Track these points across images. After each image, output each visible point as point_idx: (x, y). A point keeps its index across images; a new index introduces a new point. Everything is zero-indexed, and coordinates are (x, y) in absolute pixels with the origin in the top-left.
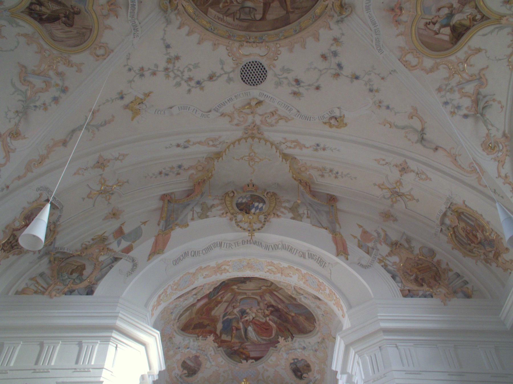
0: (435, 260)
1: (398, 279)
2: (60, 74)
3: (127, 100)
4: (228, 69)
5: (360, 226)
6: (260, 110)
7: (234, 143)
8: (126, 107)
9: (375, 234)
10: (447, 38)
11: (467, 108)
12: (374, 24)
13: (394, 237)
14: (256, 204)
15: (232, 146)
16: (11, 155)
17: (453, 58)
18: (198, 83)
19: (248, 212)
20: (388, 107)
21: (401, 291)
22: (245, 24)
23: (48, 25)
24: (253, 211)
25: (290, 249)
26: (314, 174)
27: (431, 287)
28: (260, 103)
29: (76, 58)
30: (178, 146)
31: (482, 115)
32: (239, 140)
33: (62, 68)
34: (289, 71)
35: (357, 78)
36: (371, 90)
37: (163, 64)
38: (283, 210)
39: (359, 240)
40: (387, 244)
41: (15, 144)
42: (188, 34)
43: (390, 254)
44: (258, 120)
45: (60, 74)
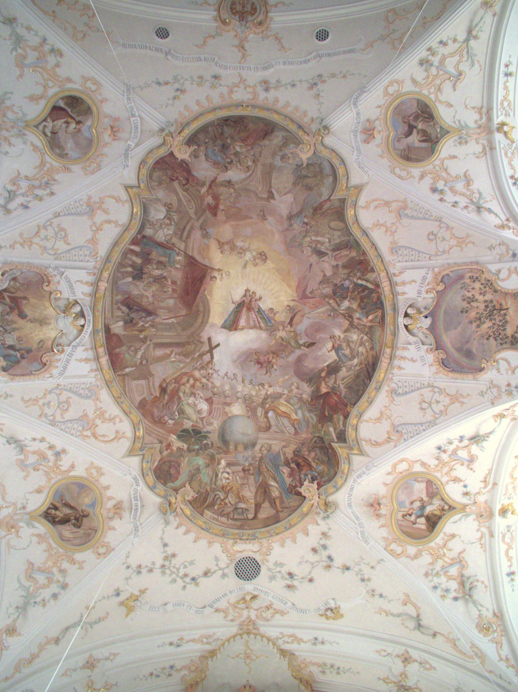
3: (123, 597)
4: (222, 565)
6: (255, 604)
7: (228, 640)
8: (122, 604)
10: (424, 527)
11: (455, 590)
12: (357, 518)
15: (227, 643)
17: (432, 544)
18: (193, 579)
20: (381, 596)
22: (238, 523)
23: (60, 527)
26: (315, 670)
28: (254, 597)
29: (79, 556)
30: (171, 644)
31: (470, 596)
32: (234, 637)
33: (65, 565)
34: (282, 565)
35: (348, 569)
36: (363, 580)
37: (159, 562)
42: (186, 533)
44: (253, 615)
45: (63, 571)
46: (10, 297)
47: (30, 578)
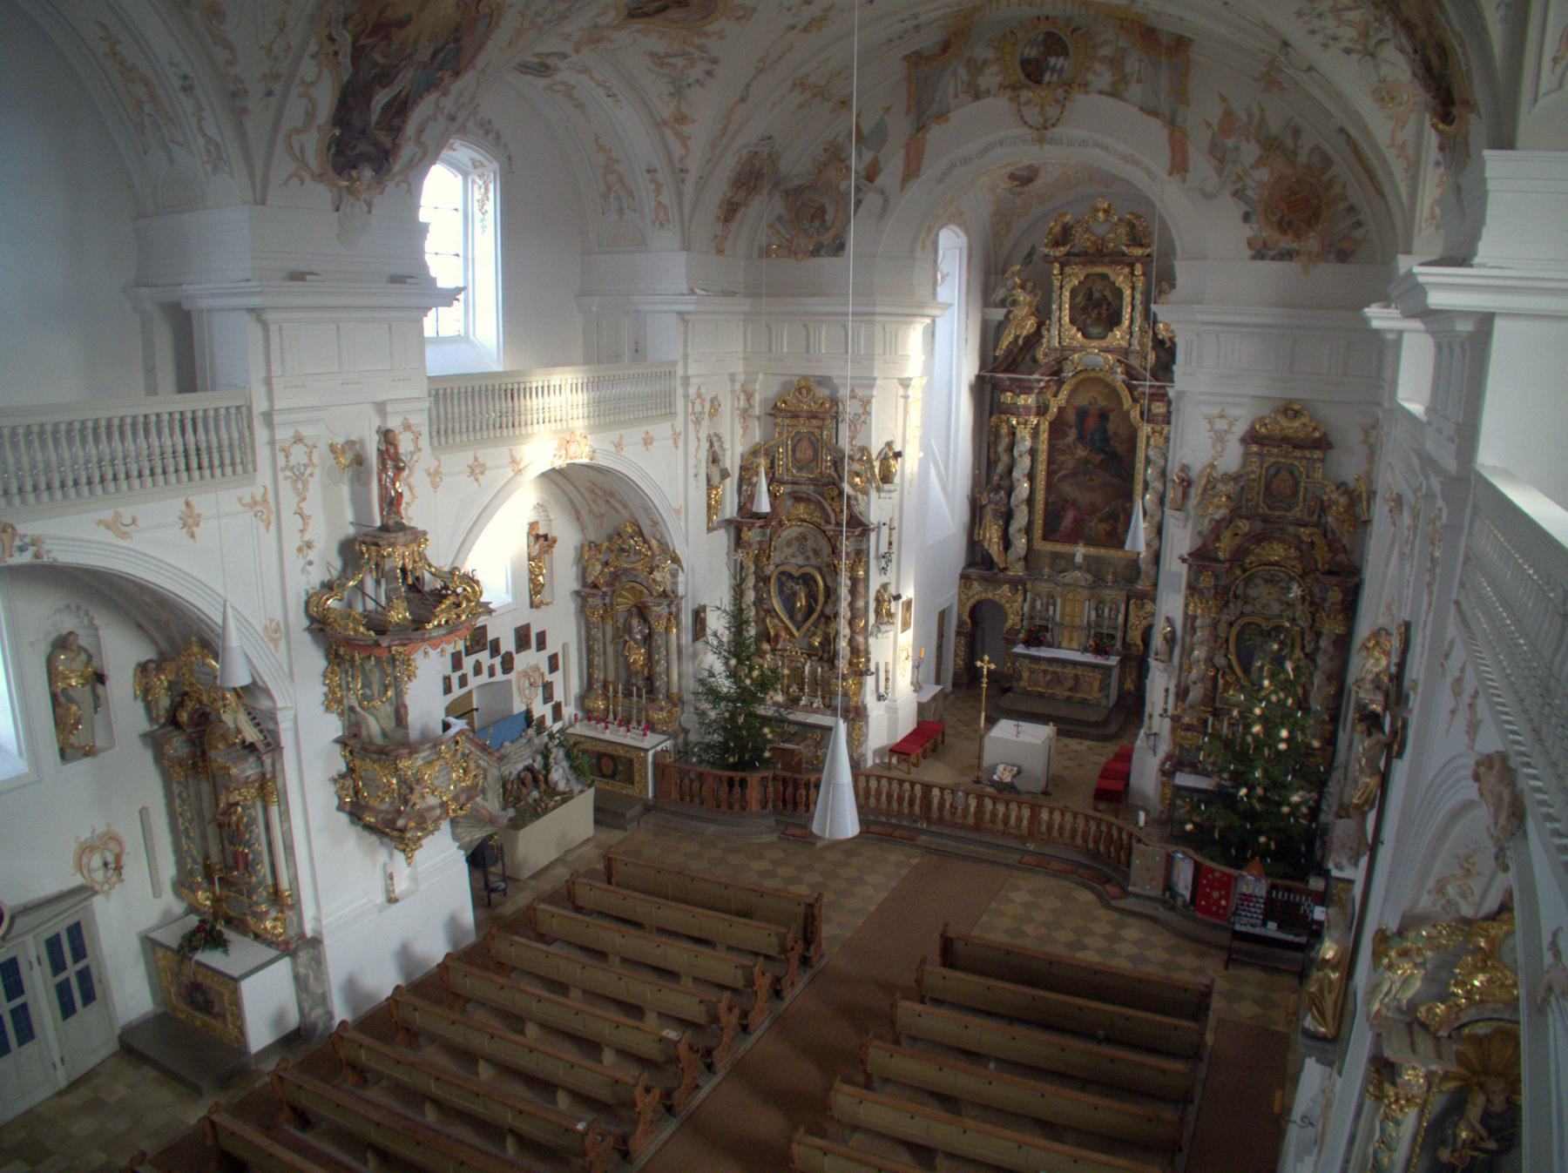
0: (1326, 178)
1: (1254, 218)
2: (702, 48)
5: (1223, 99)
9: (1244, 118)
13: (1275, 126)
14: (1053, 61)
16: (689, 142)
19: (1039, 82)
21: (1250, 244)
24: (1047, 77)
25: (1106, 149)
27: (1298, 236)
29: (711, 28)
33: (698, 41)
38: (1097, 66)
39: (1214, 134)
40: (1259, 141)
41: (686, 129)
43: (1254, 167)
46: (369, 36)
47: (662, 65)
